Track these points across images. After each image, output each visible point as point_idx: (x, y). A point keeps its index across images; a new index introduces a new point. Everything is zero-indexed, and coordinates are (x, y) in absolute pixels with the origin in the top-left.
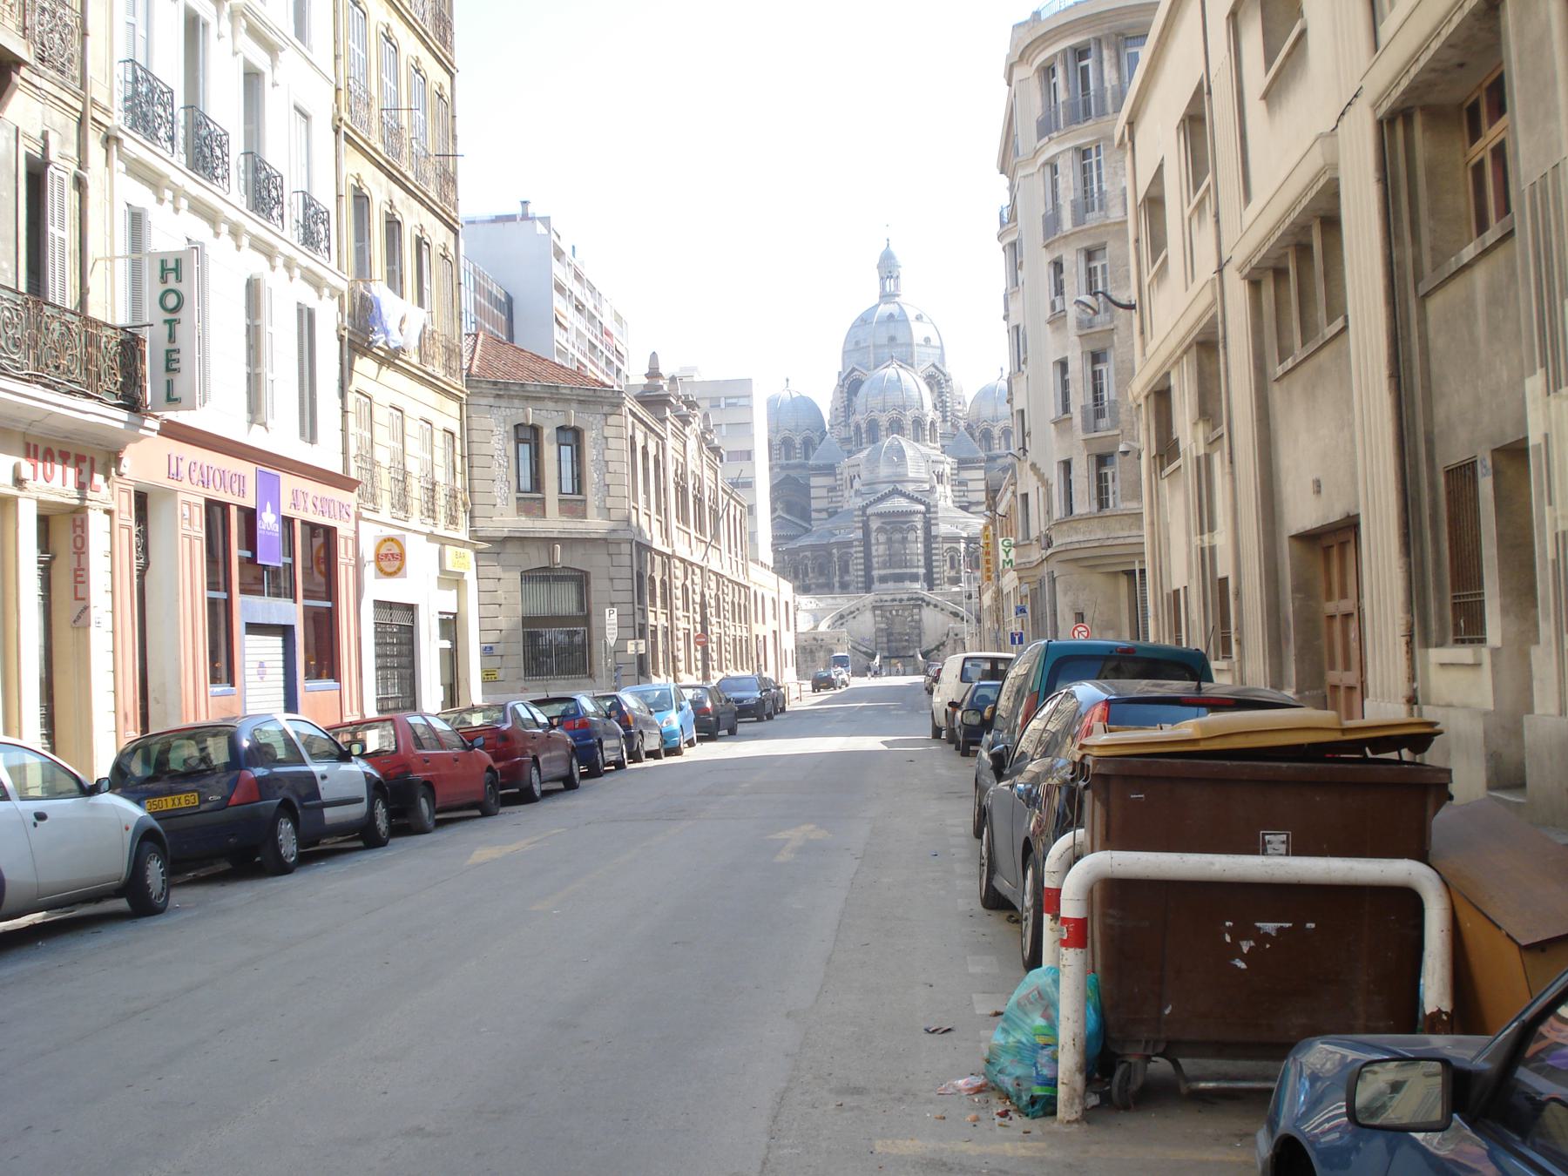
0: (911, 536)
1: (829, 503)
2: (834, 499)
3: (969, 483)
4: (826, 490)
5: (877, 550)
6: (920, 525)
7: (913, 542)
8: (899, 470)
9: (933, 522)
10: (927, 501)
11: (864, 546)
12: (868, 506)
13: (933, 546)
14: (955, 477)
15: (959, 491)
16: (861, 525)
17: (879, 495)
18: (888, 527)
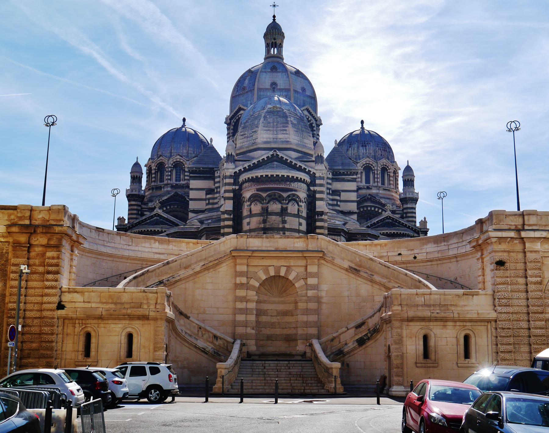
0: (292, 208)
1: (207, 204)
2: (211, 201)
3: (342, 194)
4: (204, 193)
5: (249, 224)
6: (303, 195)
8: (280, 136)
9: (318, 196)
10: (313, 171)
11: (233, 220)
13: (318, 224)
14: (329, 186)
15: (333, 200)
16: (231, 195)
17: (255, 161)
18: (264, 195)
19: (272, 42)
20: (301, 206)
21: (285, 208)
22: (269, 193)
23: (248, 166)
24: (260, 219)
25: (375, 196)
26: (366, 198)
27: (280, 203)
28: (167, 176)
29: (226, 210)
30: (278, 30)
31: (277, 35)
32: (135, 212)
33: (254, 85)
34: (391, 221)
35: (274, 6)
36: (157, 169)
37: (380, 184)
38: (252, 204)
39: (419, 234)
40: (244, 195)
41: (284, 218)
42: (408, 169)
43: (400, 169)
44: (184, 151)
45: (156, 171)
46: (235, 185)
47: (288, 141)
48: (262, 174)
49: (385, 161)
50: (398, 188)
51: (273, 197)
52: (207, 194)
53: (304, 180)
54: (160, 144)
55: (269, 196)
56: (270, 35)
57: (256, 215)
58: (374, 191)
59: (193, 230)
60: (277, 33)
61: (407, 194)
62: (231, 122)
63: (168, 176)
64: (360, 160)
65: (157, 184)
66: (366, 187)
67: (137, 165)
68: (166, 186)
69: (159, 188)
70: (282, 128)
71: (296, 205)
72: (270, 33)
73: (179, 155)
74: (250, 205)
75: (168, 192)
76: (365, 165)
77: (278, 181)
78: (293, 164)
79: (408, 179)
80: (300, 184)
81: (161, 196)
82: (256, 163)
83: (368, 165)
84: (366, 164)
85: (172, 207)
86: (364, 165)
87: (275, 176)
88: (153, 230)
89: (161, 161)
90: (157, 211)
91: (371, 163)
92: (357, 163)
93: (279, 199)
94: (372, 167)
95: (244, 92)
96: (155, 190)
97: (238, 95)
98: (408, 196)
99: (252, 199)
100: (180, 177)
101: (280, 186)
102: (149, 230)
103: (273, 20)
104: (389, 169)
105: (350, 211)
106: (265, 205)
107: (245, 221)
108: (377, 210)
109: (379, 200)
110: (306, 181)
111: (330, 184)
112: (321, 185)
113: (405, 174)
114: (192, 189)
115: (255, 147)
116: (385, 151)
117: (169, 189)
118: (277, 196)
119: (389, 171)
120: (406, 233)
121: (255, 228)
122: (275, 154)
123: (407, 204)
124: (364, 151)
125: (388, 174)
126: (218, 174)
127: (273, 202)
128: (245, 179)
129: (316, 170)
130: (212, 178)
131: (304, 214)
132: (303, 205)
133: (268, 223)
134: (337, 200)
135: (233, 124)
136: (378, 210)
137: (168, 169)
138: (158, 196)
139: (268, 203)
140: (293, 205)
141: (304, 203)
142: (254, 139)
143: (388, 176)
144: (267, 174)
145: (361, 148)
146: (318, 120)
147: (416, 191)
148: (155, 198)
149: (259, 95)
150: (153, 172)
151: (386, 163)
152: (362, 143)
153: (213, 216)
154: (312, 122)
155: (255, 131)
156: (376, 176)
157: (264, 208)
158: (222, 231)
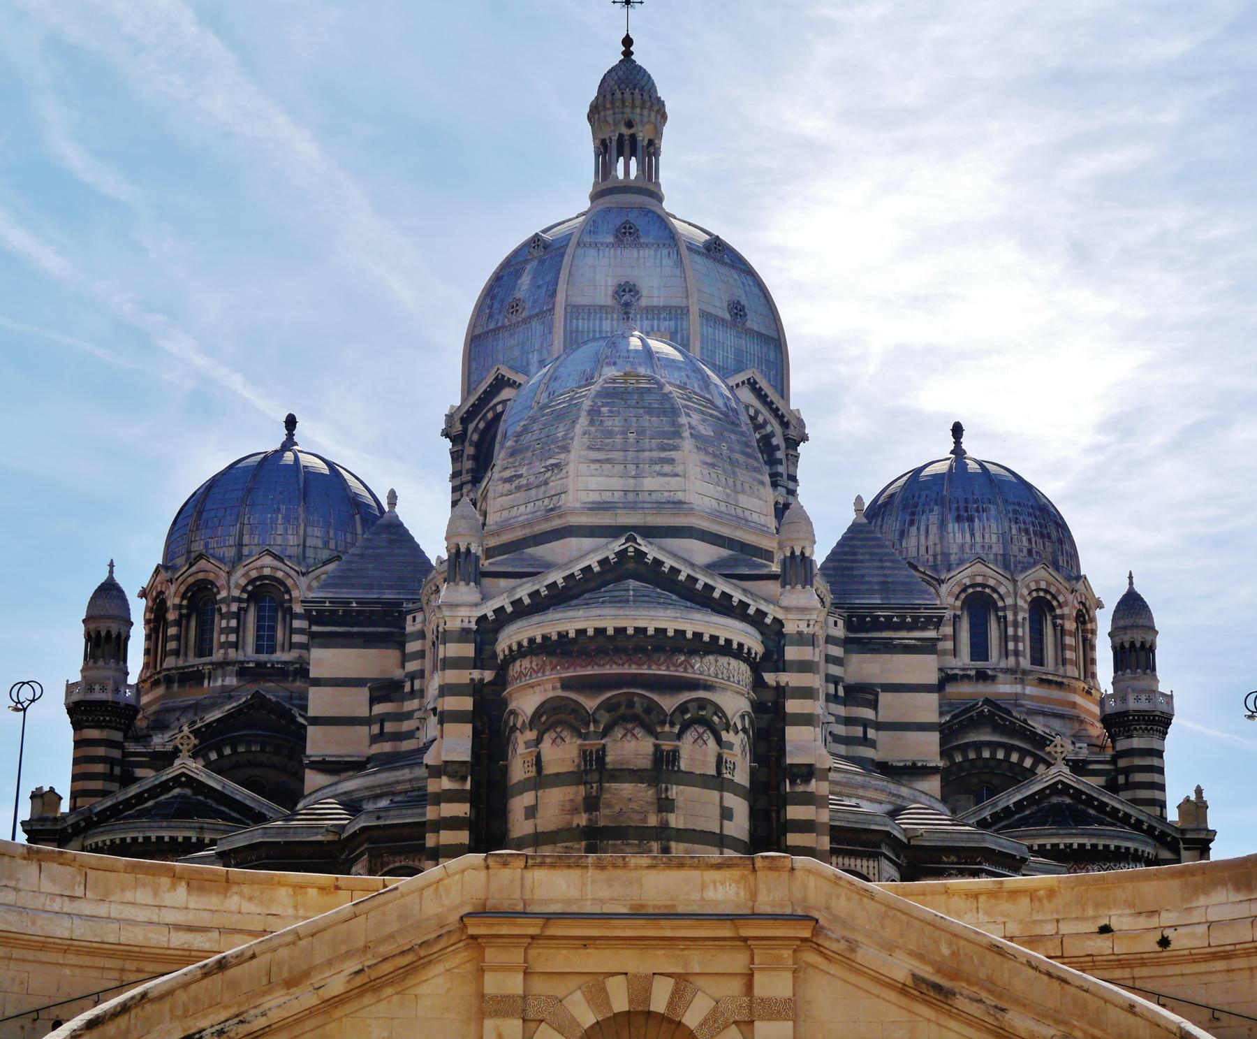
1: (374, 739)
2: (389, 727)
3: (884, 698)
4: (365, 693)
5: (531, 812)
6: (735, 704)
7: (705, 781)
8: (649, 483)
9: (792, 706)
10: (772, 612)
11: (472, 798)
12: (502, 619)
13: (794, 812)
14: (835, 670)
15: (849, 721)
16: (466, 703)
17: (557, 577)
18: (590, 703)
19: (621, 136)
20: (730, 746)
21: (668, 752)
22: (608, 695)
23: (530, 595)
24: (576, 794)
25: (1009, 707)
26: (974, 713)
27: (650, 731)
28: (222, 631)
29: (446, 762)
30: (642, 89)
31: (638, 110)
32: (100, 768)
33: (553, 294)
34: (1068, 801)
36: (188, 607)
37: (1025, 663)
38: (546, 736)
39: (1176, 851)
40: (511, 706)
41: (667, 790)
42: (1132, 606)
43: (1100, 605)
44: (291, 538)
45: (181, 615)
46: (483, 668)
47: (680, 502)
48: (580, 626)
49: (1043, 573)
50: (1094, 676)
51: (623, 710)
52: (373, 701)
53: (741, 645)
54: (200, 514)
55: (608, 706)
56: (613, 108)
57: (558, 780)
58: (1004, 688)
59: (319, 838)
60: (638, 102)
61: (1131, 698)
62: (465, 430)
63: (228, 630)
64: (949, 570)
65: (185, 660)
66: (973, 673)
67: (109, 592)
68: (220, 672)
69: (193, 678)
70: (656, 454)
71: (711, 743)
72: (612, 103)
73: (270, 553)
74: (539, 741)
75: (227, 694)
76: (970, 590)
77: (642, 650)
78: (699, 586)
79: (1132, 644)
80: (723, 660)
81: (199, 708)
82: (560, 582)
83: (979, 589)
85: (241, 749)
87: (630, 631)
88: (167, 839)
89: (201, 576)
90: (184, 765)
91: (991, 582)
92: (940, 582)
93: (645, 718)
94: (995, 596)
95: (514, 319)
96: (176, 685)
97: (494, 331)
98: (1132, 705)
99: (544, 718)
100: (272, 638)
101: (649, 668)
102: (153, 839)
103: (623, 53)
104: (1060, 606)
105: (914, 764)
106: (593, 743)
107: (518, 804)
108: (1014, 758)
109: (1025, 721)
110: (749, 649)
111: (838, 661)
112: (805, 667)
113: (1121, 623)
114: (317, 682)
115: (557, 523)
116: (1042, 536)
117: (232, 681)
118: (638, 709)
119: (1058, 612)
120: (1127, 849)
121: (555, 829)
122: (631, 549)
123: (1131, 737)
124: (964, 537)
125: (1055, 625)
126: (418, 627)
127: (623, 732)
128: (520, 644)
129: (786, 609)
130: (396, 639)
131: (741, 777)
132: (737, 740)
133: (604, 811)
134: (865, 724)
135: (475, 437)
136: (1021, 759)
137: (228, 606)
138: (189, 707)
139: (605, 734)
140: (700, 742)
141: (741, 735)
142: (553, 492)
143: (1055, 630)
144: (600, 624)
145: (952, 526)
146: (793, 422)
147: (1163, 688)
148: (178, 714)
149: (572, 331)
150: (171, 616)
151: (1048, 584)
152: (958, 509)
153: (398, 782)
154: (769, 429)
155: (557, 465)
156: (1010, 631)
157: (591, 753)
158: (430, 841)
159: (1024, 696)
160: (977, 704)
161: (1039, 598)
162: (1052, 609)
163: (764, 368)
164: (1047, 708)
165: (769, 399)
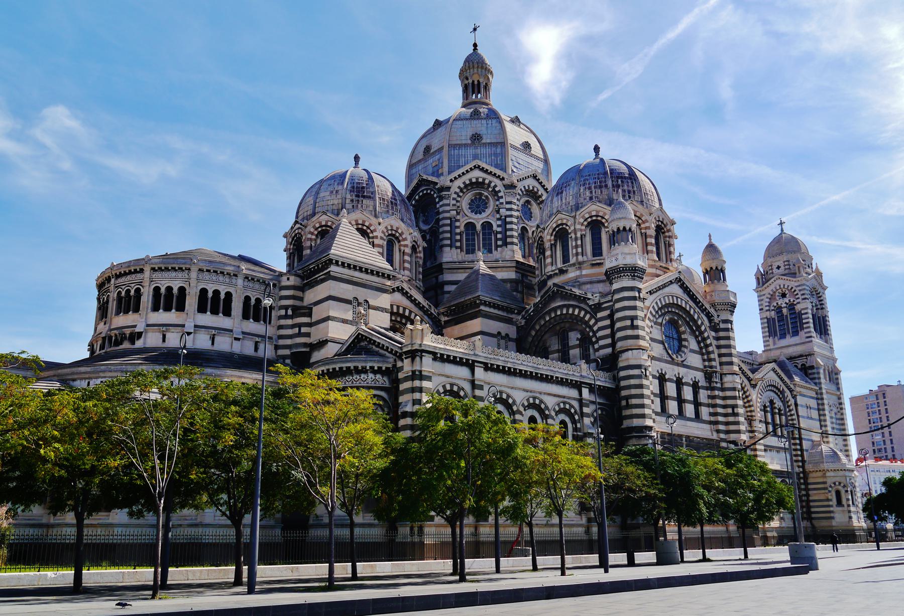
3: (315, 309)
15: (292, 326)
25: (563, 285)
26: (550, 293)
31: (468, 71)
35: (475, 29)
39: (402, 361)
66: (557, 271)
76: (557, 229)
79: (618, 229)
83: (561, 227)
84: (558, 226)
86: (554, 230)
91: (565, 221)
94: (567, 228)
103: (474, 50)
108: (571, 311)
116: (601, 187)
134: (300, 326)
145: (555, 199)
151: (597, 211)
154: (493, 185)
159: (581, 276)
160: (550, 287)
161: (592, 221)
162: (603, 224)
163: (493, 158)
164: (594, 279)
165: (489, 171)
